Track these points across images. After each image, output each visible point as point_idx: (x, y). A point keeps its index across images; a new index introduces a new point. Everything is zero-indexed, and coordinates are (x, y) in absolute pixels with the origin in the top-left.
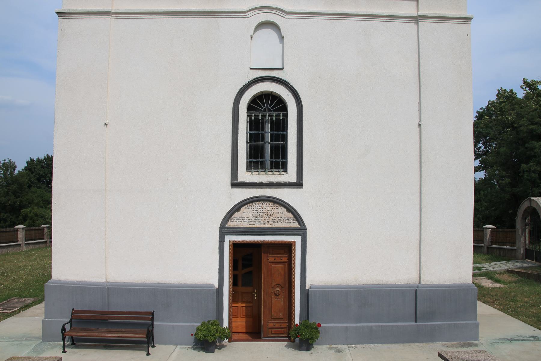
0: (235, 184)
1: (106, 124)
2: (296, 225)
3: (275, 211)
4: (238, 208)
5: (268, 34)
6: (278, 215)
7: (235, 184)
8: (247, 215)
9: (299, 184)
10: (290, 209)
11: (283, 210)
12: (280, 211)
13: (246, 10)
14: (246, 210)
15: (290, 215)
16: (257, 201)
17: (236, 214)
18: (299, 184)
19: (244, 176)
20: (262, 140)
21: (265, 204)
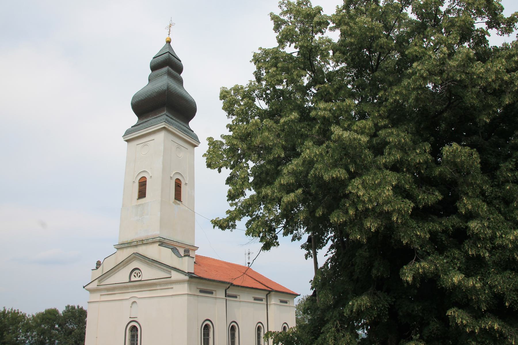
1: (97, 337)
5: (134, 305)
13: (128, 298)
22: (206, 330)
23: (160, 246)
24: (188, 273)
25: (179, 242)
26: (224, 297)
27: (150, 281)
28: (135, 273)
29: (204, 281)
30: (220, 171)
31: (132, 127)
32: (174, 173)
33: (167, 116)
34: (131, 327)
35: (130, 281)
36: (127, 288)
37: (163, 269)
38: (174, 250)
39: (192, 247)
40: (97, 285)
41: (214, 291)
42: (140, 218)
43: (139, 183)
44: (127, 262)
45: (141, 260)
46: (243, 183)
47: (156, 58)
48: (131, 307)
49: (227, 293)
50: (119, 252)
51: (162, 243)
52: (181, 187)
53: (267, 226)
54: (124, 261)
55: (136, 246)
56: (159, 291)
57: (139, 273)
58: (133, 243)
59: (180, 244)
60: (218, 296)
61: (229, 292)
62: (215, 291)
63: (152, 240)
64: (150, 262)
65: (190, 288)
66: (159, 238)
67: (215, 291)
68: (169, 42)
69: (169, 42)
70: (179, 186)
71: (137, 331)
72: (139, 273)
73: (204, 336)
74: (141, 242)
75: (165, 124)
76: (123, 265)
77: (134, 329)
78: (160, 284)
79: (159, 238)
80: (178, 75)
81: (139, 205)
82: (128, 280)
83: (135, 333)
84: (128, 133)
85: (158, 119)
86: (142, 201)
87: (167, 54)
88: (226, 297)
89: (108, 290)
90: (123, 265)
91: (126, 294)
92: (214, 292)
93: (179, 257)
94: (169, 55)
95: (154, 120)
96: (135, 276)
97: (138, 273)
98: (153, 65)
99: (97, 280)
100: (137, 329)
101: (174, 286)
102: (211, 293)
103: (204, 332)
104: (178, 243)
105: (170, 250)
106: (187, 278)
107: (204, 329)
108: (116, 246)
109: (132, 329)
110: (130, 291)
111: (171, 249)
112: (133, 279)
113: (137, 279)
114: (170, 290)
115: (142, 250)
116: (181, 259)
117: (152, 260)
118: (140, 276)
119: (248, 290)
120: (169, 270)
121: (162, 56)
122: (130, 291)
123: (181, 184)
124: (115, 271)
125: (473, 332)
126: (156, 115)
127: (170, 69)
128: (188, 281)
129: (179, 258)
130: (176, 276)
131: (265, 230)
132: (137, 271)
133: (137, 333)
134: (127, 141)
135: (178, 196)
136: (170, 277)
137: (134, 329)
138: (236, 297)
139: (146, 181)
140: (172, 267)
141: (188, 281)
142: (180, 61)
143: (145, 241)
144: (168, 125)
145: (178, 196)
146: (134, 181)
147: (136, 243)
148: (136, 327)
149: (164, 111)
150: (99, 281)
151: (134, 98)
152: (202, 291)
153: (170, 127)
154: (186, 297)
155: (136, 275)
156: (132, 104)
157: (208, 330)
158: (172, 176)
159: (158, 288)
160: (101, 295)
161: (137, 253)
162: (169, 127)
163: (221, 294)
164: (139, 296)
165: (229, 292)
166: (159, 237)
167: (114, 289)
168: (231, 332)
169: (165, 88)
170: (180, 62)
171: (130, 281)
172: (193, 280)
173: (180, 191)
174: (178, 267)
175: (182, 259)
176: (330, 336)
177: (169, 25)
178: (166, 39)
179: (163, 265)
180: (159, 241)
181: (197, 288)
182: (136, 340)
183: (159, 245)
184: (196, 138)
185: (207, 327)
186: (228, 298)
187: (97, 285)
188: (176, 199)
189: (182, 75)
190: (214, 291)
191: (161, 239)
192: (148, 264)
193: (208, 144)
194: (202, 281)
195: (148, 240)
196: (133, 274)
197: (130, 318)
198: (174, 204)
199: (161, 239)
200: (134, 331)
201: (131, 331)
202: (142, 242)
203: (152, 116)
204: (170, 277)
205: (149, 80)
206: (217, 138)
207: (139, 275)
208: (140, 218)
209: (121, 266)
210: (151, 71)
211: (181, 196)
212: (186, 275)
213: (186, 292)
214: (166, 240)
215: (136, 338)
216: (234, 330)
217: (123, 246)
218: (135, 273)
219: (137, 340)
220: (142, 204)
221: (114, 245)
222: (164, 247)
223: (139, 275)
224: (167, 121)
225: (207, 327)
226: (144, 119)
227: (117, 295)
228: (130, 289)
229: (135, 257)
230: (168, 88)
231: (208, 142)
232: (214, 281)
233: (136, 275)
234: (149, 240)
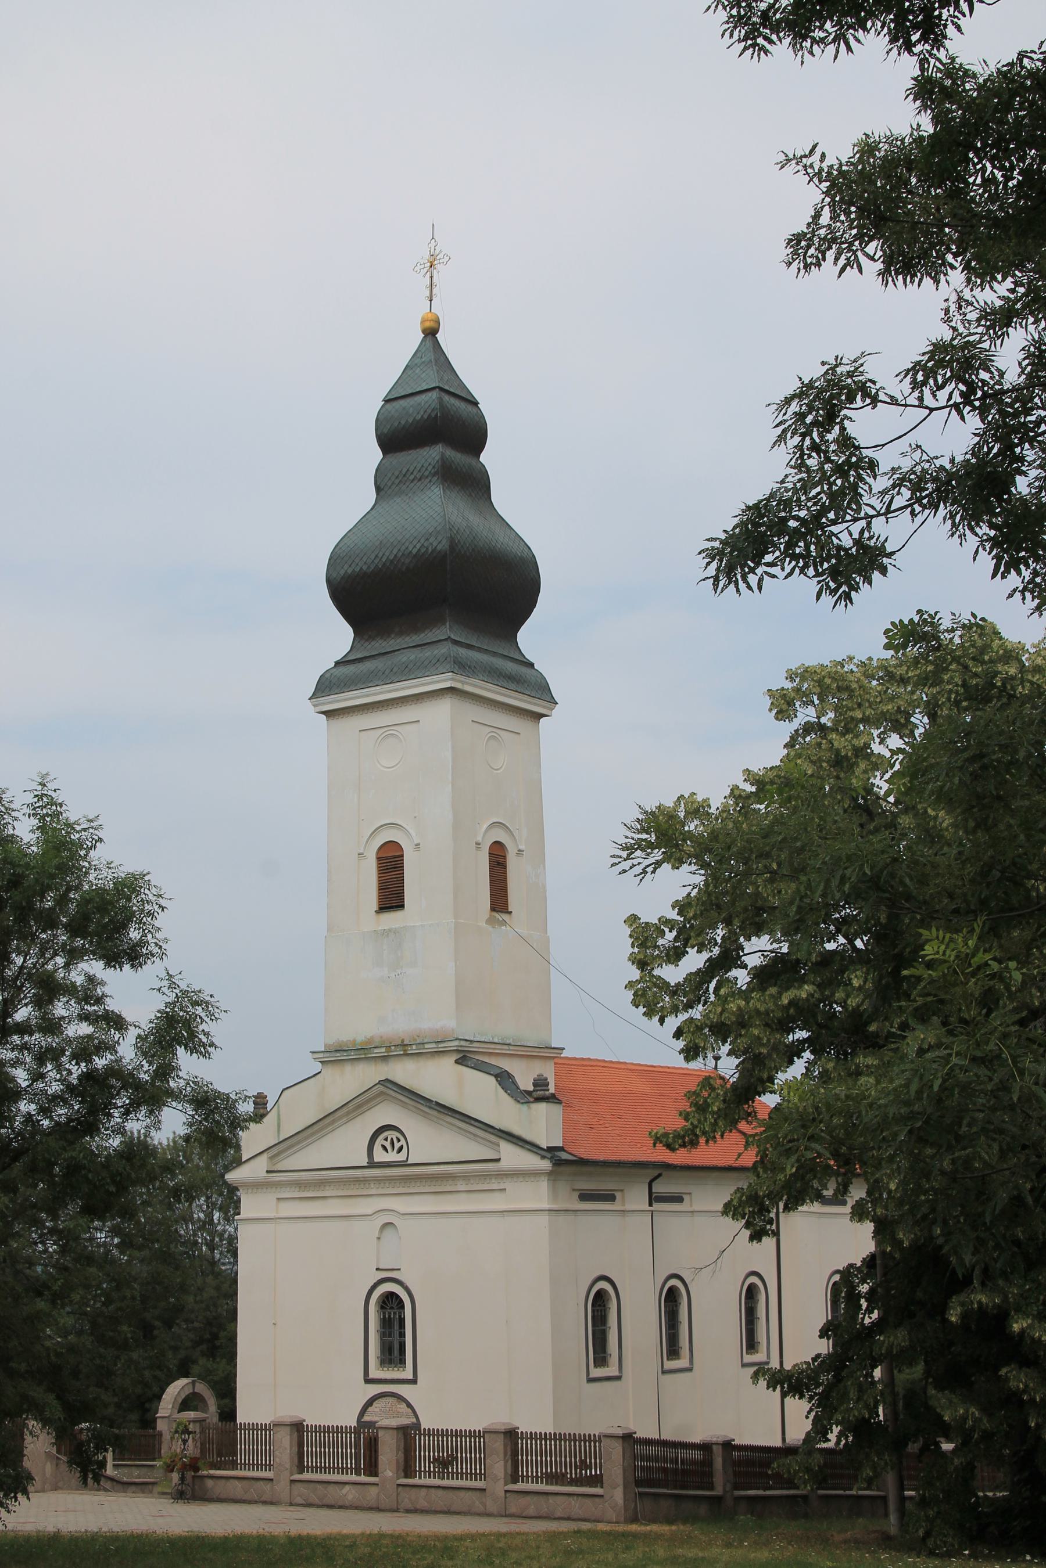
0: (368, 1381)
1: (274, 1324)
2: (414, 1420)
3: (398, 1406)
4: (370, 1403)
5: (389, 1232)
6: (400, 1410)
7: (368, 1381)
8: (378, 1410)
9: (414, 1381)
10: (409, 1405)
11: (404, 1405)
12: (402, 1406)
13: (370, 1211)
14: (377, 1405)
15: (409, 1410)
16: (384, 1396)
17: (370, 1409)
18: (414, 1381)
19: (374, 1373)
20: (390, 1336)
21: (391, 1400)
22: (600, 1306)
23: (460, 1067)
24: (550, 1149)
25: (509, 1045)
26: (647, 1207)
27: (436, 1167)
28: (386, 1139)
29: (591, 1169)
30: (662, 1021)
31: (337, 663)
32: (485, 826)
33: (456, 643)
34: (382, 1295)
35: (372, 1165)
36: (364, 1181)
37: (475, 1135)
38: (504, 1079)
39: (546, 1050)
40: (268, 1172)
41: (616, 1190)
42: (392, 975)
43: (379, 859)
44: (359, 1106)
45: (403, 1105)
46: (715, 1121)
47: (397, 405)
48: (379, 1238)
49: (653, 1191)
50: (330, 1074)
51: (464, 1059)
52: (505, 867)
53: (756, 1203)
54: (350, 1104)
55: (384, 1058)
56: (464, 1196)
57: (399, 1140)
58: (376, 1051)
59: (512, 1048)
60: (628, 1207)
61: (659, 1188)
62: (622, 1191)
63: (434, 1045)
64: (435, 1113)
65: (554, 1195)
66: (456, 1043)
67: (622, 1191)
68: (431, 333)
69: (431, 333)
70: (499, 863)
71: (403, 1307)
72: (399, 1140)
73: (593, 1325)
74: (401, 1048)
75: (452, 679)
76: (348, 1113)
77: (391, 1304)
78: (466, 1177)
79: (456, 1043)
80: (473, 462)
81: (386, 933)
82: (364, 1161)
83: (395, 1313)
84: (325, 686)
85: (427, 653)
86: (392, 919)
87: (434, 394)
88: (650, 1205)
89: (299, 1185)
90: (348, 1113)
91: (360, 1200)
92: (618, 1195)
93: (519, 1101)
94: (440, 399)
95: (412, 655)
96: (385, 1148)
97: (395, 1141)
98: (385, 431)
99: (265, 1156)
100: (401, 1301)
101: (508, 1184)
102: (610, 1198)
103: (593, 1311)
104: (506, 1047)
105: (493, 1079)
106: (546, 1165)
107: (593, 1305)
108: (321, 1055)
109: (384, 1302)
110: (373, 1192)
111: (496, 1076)
112: (379, 1156)
113: (392, 1156)
114: (497, 1194)
115: (403, 1072)
116: (525, 1106)
117: (438, 1104)
118: (400, 1149)
119: (715, 1174)
120: (493, 1138)
121: (418, 399)
122: (373, 1192)
123: (504, 857)
124: (322, 1129)
125: (1032, 1400)
126: (416, 629)
127: (451, 453)
128: (550, 1174)
129: (519, 1106)
130: (512, 1156)
131: (754, 1211)
132: (392, 1135)
133: (400, 1313)
134: (328, 714)
135: (499, 901)
136: (498, 1160)
137: (391, 1304)
138: (678, 1199)
139: (403, 856)
140: (500, 1130)
141: (550, 1174)
142: (475, 404)
143: (414, 1047)
144: (462, 678)
145: (499, 901)
146: (361, 851)
147: (383, 1050)
148: (397, 1296)
149: (439, 621)
150: (271, 1158)
151: (335, 560)
152: (585, 1197)
153: (468, 684)
154: (544, 1220)
155: (388, 1145)
156: (329, 582)
157: (604, 1306)
158: (479, 839)
159: (462, 1186)
160: (278, 1199)
161: (387, 1080)
162: (463, 683)
163: (636, 1197)
164: (402, 1209)
165: (659, 1188)
166: (457, 1039)
167: (321, 1183)
168: (665, 1307)
169: (443, 545)
170: (475, 410)
171: (372, 1165)
172: (562, 1169)
173: (505, 880)
174: (517, 1130)
175: (529, 1108)
176: (852, 1384)
177: (427, 256)
178: (423, 321)
179: (473, 1122)
180: (457, 1051)
181: (574, 1190)
182: (397, 1334)
183: (457, 1062)
184: (542, 690)
185: (600, 1300)
186: (656, 1206)
187: (268, 1172)
188: (493, 909)
189: (483, 458)
190: (616, 1190)
191: (463, 1043)
192: (425, 1115)
193: (631, 936)
194: (585, 1169)
195: (421, 1046)
196: (380, 1141)
197: (377, 1269)
198: (489, 928)
199: (463, 1043)
200: (392, 1308)
201: (382, 1307)
202: (405, 1051)
203: (401, 633)
204: (498, 1160)
205: (378, 489)
206: (650, 917)
207: (397, 1145)
208: (392, 975)
209: (340, 1118)
210: (379, 454)
211: (506, 896)
212: (543, 1157)
213: (546, 1206)
214: (475, 1045)
215: (396, 1327)
216: (676, 1301)
217: (339, 1056)
218: (386, 1139)
219: (402, 1335)
220: (395, 932)
221: (313, 1053)
222: (472, 1068)
223: (397, 1145)
224: (462, 667)
225: (600, 1300)
226: (372, 638)
227: (330, 1201)
228: (372, 1185)
229: (382, 1093)
230: (453, 543)
231: (628, 931)
232: (619, 1164)
233: (388, 1145)
234: (426, 1046)
